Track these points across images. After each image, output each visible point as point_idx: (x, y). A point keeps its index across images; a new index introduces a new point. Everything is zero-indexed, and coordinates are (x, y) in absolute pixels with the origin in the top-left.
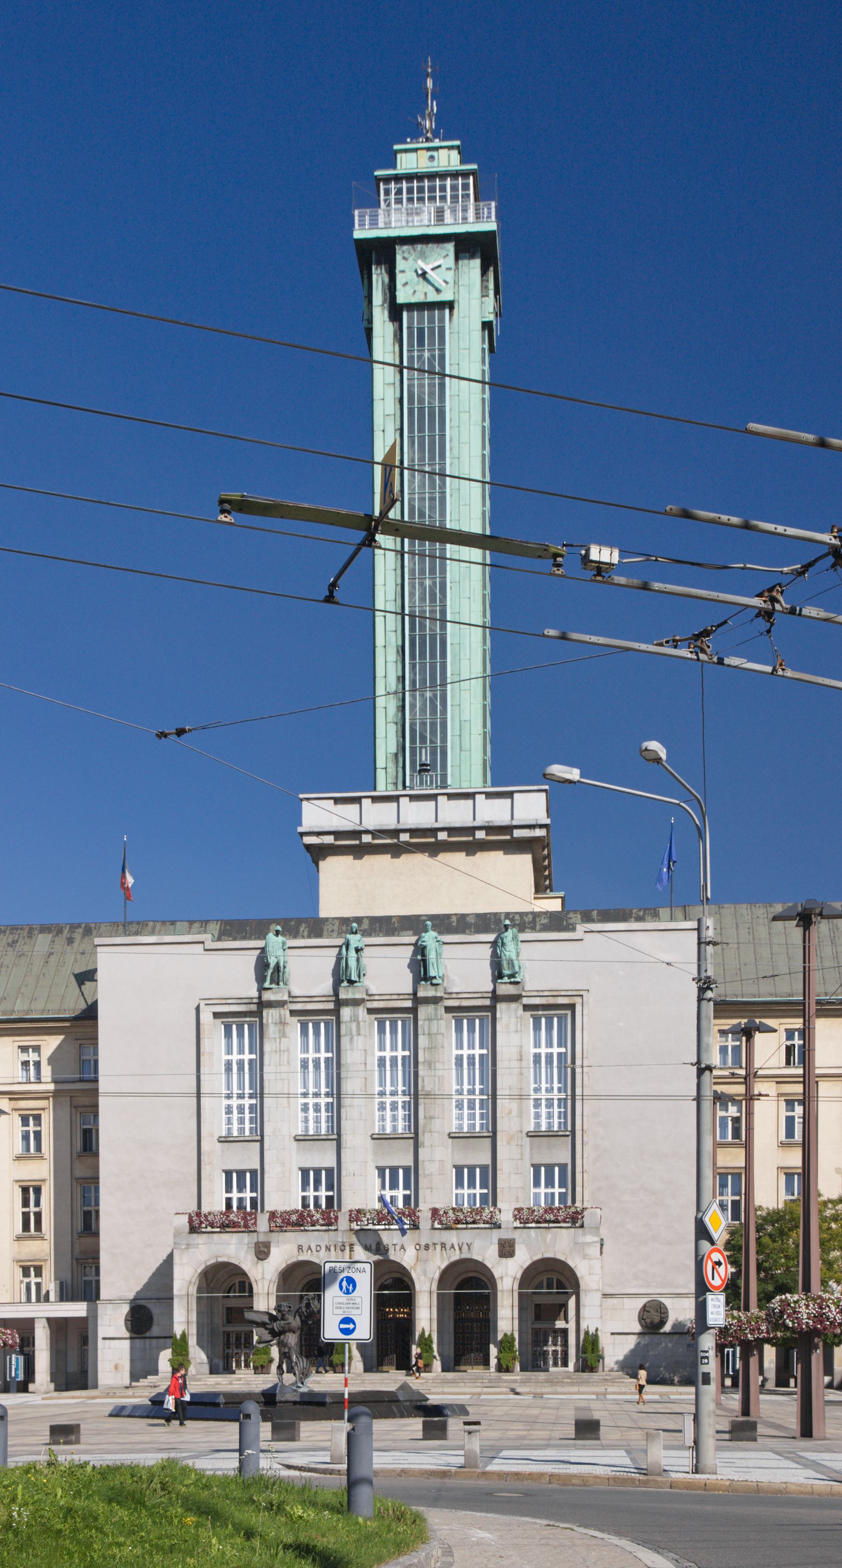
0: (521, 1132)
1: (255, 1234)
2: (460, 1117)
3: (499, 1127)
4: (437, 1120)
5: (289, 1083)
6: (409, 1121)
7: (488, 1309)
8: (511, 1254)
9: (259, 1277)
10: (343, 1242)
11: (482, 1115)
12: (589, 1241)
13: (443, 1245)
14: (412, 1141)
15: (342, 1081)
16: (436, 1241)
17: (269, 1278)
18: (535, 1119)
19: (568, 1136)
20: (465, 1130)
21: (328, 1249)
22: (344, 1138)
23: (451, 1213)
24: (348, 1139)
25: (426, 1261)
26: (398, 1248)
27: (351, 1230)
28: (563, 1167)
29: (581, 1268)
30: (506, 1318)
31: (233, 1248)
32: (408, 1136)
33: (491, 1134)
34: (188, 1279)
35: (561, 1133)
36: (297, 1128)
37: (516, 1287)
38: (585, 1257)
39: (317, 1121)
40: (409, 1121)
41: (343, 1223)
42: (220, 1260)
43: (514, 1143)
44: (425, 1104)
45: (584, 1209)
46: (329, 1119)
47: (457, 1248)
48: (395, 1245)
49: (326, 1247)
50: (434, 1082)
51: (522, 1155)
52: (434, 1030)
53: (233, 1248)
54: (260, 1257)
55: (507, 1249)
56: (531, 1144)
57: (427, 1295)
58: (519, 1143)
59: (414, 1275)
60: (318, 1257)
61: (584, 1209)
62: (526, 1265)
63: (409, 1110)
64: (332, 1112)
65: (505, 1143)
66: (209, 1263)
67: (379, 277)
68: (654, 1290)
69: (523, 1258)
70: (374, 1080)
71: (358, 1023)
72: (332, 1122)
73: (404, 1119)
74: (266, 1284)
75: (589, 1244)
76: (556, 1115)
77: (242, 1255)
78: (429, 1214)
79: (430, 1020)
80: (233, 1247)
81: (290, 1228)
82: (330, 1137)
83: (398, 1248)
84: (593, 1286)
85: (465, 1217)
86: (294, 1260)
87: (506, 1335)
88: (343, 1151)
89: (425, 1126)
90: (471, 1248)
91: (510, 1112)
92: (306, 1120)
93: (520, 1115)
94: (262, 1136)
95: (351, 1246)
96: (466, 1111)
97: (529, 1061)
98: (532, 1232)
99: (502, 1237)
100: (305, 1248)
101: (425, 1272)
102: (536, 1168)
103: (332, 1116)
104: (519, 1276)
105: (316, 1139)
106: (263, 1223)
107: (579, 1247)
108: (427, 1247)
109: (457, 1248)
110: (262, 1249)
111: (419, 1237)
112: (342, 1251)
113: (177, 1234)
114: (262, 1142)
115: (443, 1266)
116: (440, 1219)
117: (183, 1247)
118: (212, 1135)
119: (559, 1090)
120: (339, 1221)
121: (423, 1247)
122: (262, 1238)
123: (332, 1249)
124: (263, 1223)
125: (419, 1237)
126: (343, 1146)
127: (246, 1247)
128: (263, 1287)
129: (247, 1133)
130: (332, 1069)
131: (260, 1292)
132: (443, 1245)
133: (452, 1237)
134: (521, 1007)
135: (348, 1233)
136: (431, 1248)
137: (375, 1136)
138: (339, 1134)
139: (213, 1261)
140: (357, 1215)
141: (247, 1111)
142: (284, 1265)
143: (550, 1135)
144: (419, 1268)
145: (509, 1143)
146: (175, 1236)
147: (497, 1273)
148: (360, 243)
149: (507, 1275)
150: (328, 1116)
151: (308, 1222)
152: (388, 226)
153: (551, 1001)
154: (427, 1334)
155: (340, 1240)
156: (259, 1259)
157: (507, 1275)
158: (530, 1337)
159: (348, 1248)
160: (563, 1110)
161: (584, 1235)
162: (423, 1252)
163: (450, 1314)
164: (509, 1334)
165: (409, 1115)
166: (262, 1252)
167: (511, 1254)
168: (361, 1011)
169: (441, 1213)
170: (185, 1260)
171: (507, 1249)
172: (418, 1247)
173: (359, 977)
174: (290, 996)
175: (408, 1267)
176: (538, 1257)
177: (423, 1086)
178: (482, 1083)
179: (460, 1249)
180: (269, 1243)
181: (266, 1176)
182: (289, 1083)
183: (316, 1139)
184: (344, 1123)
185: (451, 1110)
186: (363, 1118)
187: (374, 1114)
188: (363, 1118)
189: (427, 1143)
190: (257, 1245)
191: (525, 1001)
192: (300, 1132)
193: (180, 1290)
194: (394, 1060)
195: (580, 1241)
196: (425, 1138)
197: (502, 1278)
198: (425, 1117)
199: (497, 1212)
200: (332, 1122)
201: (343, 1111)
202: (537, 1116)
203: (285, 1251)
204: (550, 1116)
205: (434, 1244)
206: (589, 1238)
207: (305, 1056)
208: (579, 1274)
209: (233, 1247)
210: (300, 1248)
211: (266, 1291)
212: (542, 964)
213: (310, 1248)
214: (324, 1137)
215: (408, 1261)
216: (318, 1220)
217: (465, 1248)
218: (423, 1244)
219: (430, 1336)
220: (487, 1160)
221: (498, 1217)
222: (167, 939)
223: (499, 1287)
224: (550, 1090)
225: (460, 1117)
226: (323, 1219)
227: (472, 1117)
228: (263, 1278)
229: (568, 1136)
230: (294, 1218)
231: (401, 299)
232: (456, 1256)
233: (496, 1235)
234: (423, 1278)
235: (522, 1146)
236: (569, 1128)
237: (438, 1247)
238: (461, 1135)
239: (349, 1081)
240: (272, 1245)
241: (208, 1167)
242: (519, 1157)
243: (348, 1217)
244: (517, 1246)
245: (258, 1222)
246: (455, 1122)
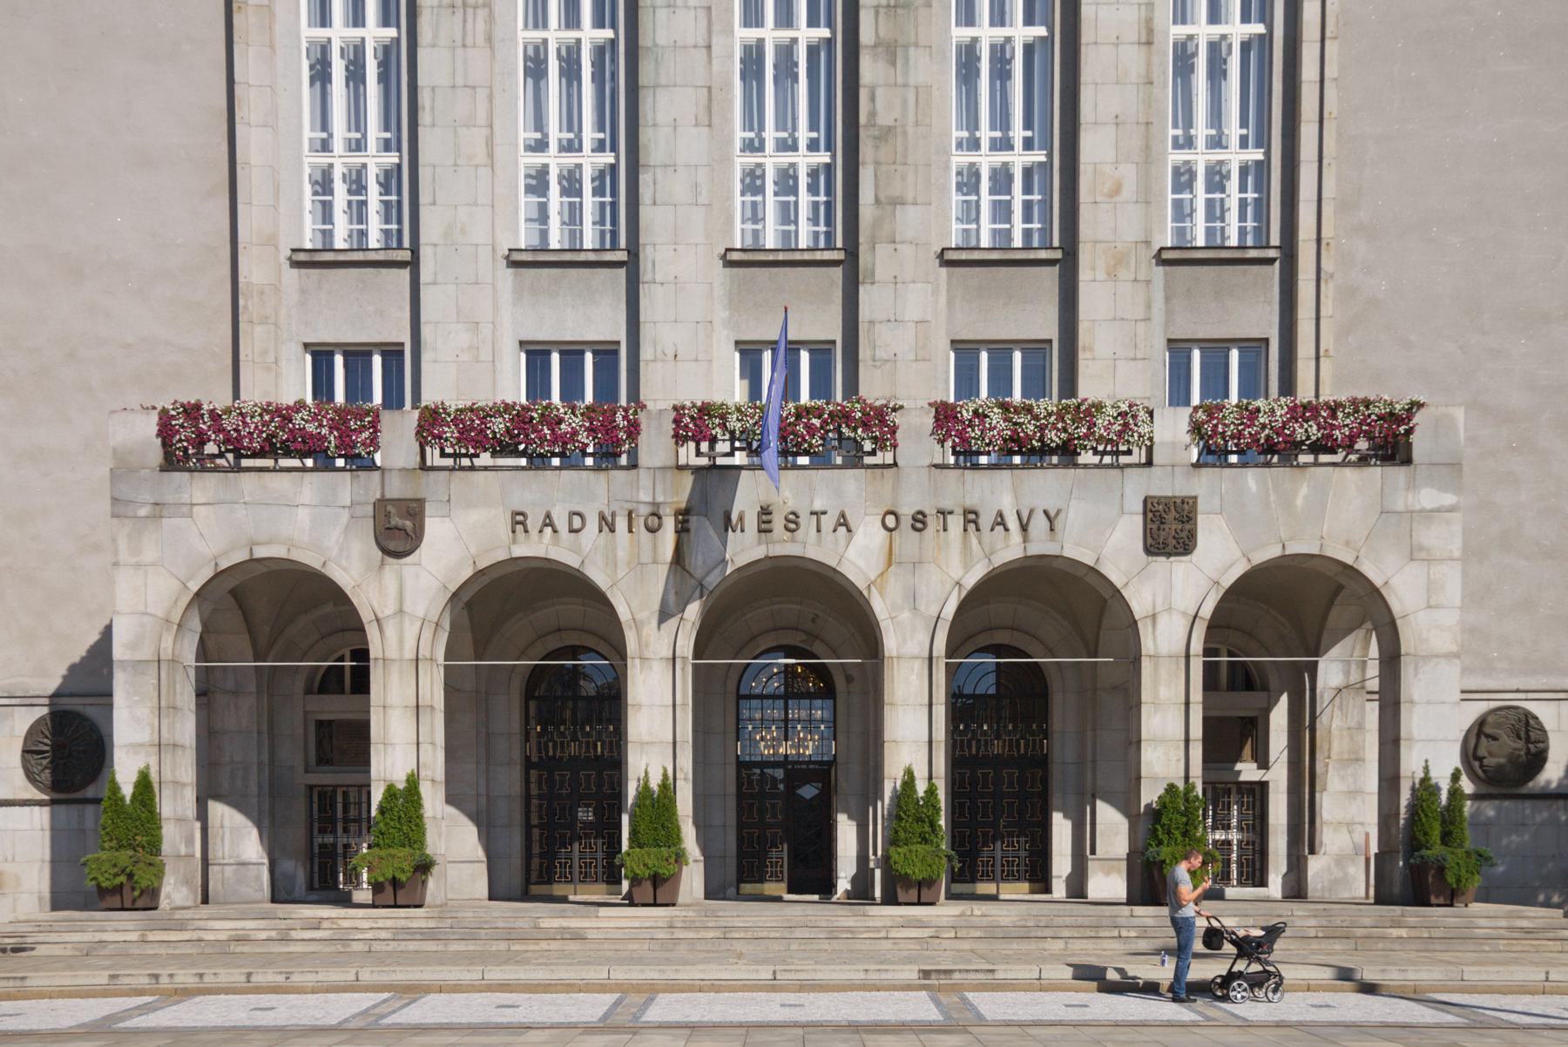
0: (1147, 243)
1: (377, 474)
2: (971, 213)
3: (1085, 230)
4: (911, 211)
5: (491, 97)
6: (829, 221)
8: (1184, 544)
9: (387, 610)
10: (655, 504)
11: (1028, 206)
12: (1428, 506)
13: (971, 517)
14: (838, 273)
15: (642, 93)
16: (947, 504)
17: (421, 613)
18: (1175, 220)
19: (1271, 261)
20: (985, 242)
21: (607, 524)
22: (647, 255)
23: (996, 417)
24: (658, 258)
25: (917, 564)
26: (828, 522)
27: (680, 468)
28: (1254, 348)
30: (1163, 741)
31: (304, 519)
32: (827, 255)
33: (1058, 255)
34: (160, 613)
35: (1253, 254)
36: (516, 232)
37: (1197, 646)
38: (1414, 553)
39: (573, 216)
40: (829, 221)
41: (655, 445)
42: (261, 552)
43: (1123, 274)
44: (877, 163)
45: (1416, 405)
46: (607, 214)
47: (1013, 523)
48: (817, 514)
49: (602, 517)
50: (905, 102)
51: (1149, 306)
53: (304, 519)
54: (392, 546)
55: (1169, 530)
56: (1168, 287)
57: (920, 667)
58: (1141, 277)
59: (879, 607)
60: (576, 549)
61: (1416, 405)
62: (1228, 580)
63: (830, 191)
64: (614, 193)
65: (1101, 275)
66: (224, 565)
69: (1220, 557)
70: (731, 102)
72: (614, 222)
73: (814, 220)
74: (411, 631)
75: (1428, 515)
76: (1233, 204)
77: (333, 538)
78: (929, 420)
80: (303, 515)
81: (485, 459)
82: (609, 257)
83: (828, 522)
85: (1042, 428)
86: (502, 556)
87: (1171, 789)
88: (644, 290)
89: (877, 223)
90: (1058, 524)
91: (1117, 190)
92: (543, 215)
93: (1147, 198)
94: (415, 251)
96: (986, 199)
97: (1165, 54)
99: (1155, 492)
100: (534, 522)
101: (913, 598)
102: (1178, 349)
103: (614, 205)
104: (1207, 611)
105: (570, 262)
107: (1402, 526)
109: (1013, 523)
110: (396, 521)
111: (895, 488)
112: (652, 530)
113: (122, 470)
114: (414, 264)
115: (971, 581)
116: (960, 434)
117: (143, 512)
118: (271, 242)
119: (1244, 142)
120: (643, 439)
121: (906, 522)
122: (397, 488)
123: (621, 524)
125: (895, 488)
126: (646, 274)
127: (345, 515)
128: (401, 641)
129: (374, 240)
130: (614, 76)
131: (392, 653)
132: (971, 517)
133: (999, 491)
135: (669, 474)
136: (933, 523)
137: (735, 256)
138: (634, 250)
139: (240, 556)
140: (696, 423)
141: (373, 190)
142: (467, 573)
143: (1218, 258)
144: (895, 585)
145: (1112, 275)
146: (115, 476)
147: (1139, 604)
149: (1171, 605)
150: (602, 205)
151: (542, 438)
154: (921, 788)
155: (645, 496)
156: (386, 552)
157: (1171, 605)
160: (1251, 195)
161: (1412, 486)
162: (907, 540)
164: (1181, 785)
165: (829, 206)
166: (397, 532)
167: (1184, 544)
169: (967, 415)
170: (149, 555)
171: (1169, 530)
172: (891, 520)
175: (861, 584)
176: (1273, 552)
177: (873, 114)
178: (1028, 125)
179: (1024, 528)
180: (421, 502)
181: (426, 357)
182: (491, 97)
183: (570, 262)
184: (645, 212)
185: (945, 189)
186: (703, 199)
187: (730, 197)
188: (703, 199)
189: (879, 275)
190: (381, 505)
192: (524, 237)
194: (786, 53)
195: (1400, 506)
196: (877, 259)
197: (1154, 617)
198: (877, 201)
199: (1142, 415)
200: (614, 222)
201: (645, 178)
202: (1182, 212)
203: (469, 527)
204: (1215, 212)
205: (943, 513)
206: (1428, 497)
207: (538, 35)
208: (1396, 608)
209: (303, 515)
210: (519, 520)
211: (409, 654)
213: (548, 521)
214: (592, 257)
215: (861, 563)
216: (575, 433)
217: (1039, 525)
218: (907, 511)
219: (931, 791)
220: (1043, 324)
221: (1144, 429)
223: (1147, 645)
224: (1217, 142)
225: (971, 213)
226: (591, 430)
227: (1002, 211)
228: (401, 611)
229: (1271, 261)
230: (499, 425)
232: (1010, 550)
233: (1137, 487)
234: (905, 615)
235: (1148, 282)
236: (1275, 240)
237: (955, 522)
238: (976, 256)
239: (663, 97)
240: (429, 509)
241: (258, 329)
242: (1140, 312)
243: (669, 427)
244: (1200, 518)
245: (384, 438)
246: (956, 227)
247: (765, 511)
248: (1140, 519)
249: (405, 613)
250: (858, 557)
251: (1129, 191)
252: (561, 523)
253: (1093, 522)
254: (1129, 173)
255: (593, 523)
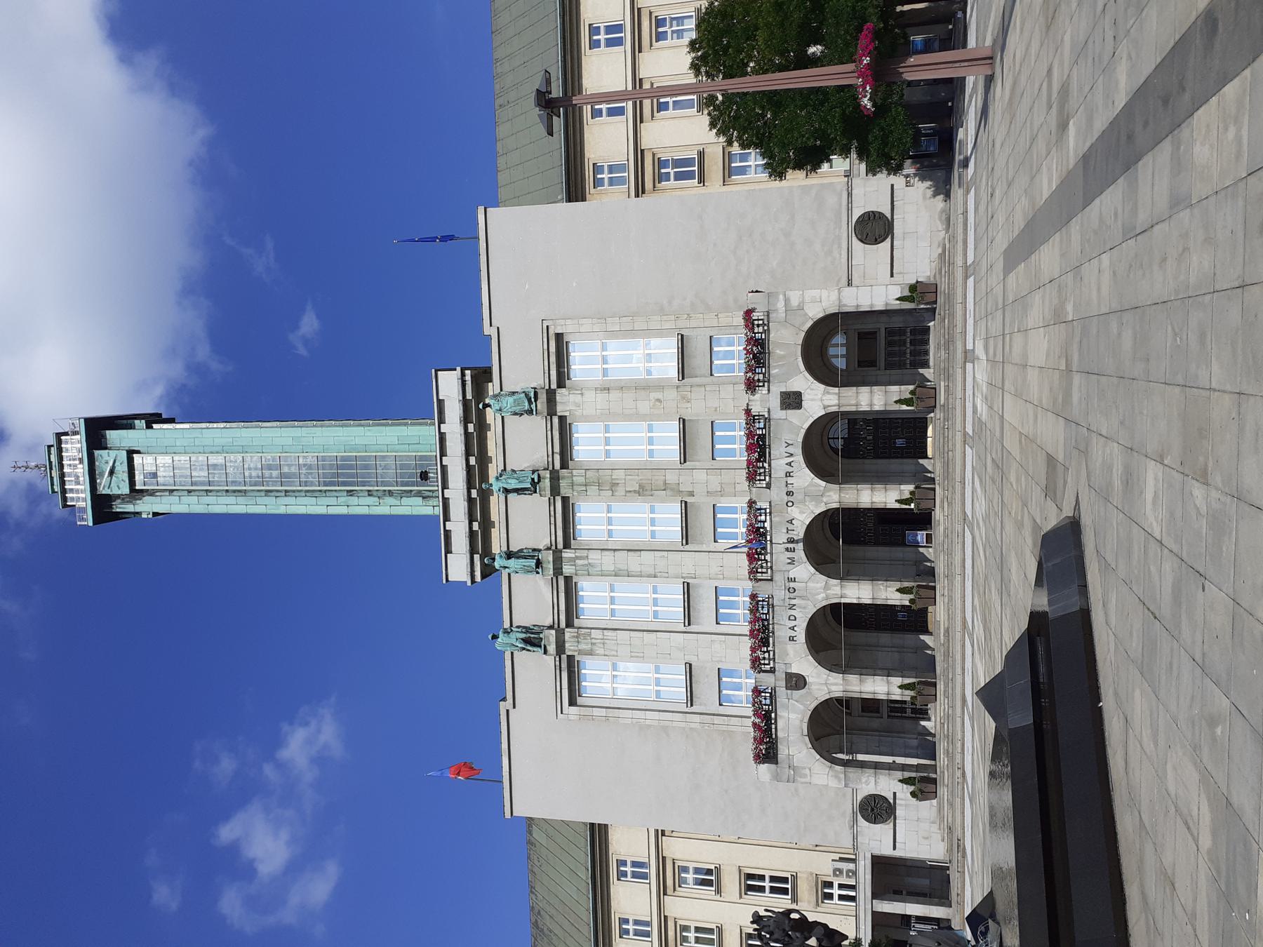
7: (864, 420)
13: (788, 475)
21: (792, 607)
29: (815, 312)
52: (582, 480)
55: (792, 401)
67: (119, 507)
68: (844, 230)
69: (803, 382)
71: (577, 558)
79: (573, 484)
80: (792, 716)
84: (834, 296)
91: (659, 400)
95: (790, 580)
98: (773, 372)
100: (792, 633)
106: (767, 680)
108: (789, 493)
121: (791, 498)
124: (767, 680)
131: (841, 688)
132: (788, 475)
133: (778, 464)
134: (559, 391)
148: (94, 523)
152: (85, 500)
153: (553, 359)
158: (893, 372)
159: (792, 585)
161: (776, 310)
162: (797, 497)
163: (870, 464)
166: (796, 682)
168: (567, 554)
173: (533, 557)
174: (551, 627)
191: (554, 386)
193: (839, 780)
203: (795, 655)
208: (821, 315)
209: (792, 716)
210: (792, 639)
212: (520, 368)
213: (792, 628)
218: (786, 498)
222: (504, 746)
223: (835, 409)
231: (126, 490)
237: (790, 480)
247: (787, 549)
248: (789, 411)
249: (826, 684)
250: (802, 516)
251: (659, 395)
252: (793, 623)
253: (790, 430)
254: (654, 395)
255: (792, 612)
